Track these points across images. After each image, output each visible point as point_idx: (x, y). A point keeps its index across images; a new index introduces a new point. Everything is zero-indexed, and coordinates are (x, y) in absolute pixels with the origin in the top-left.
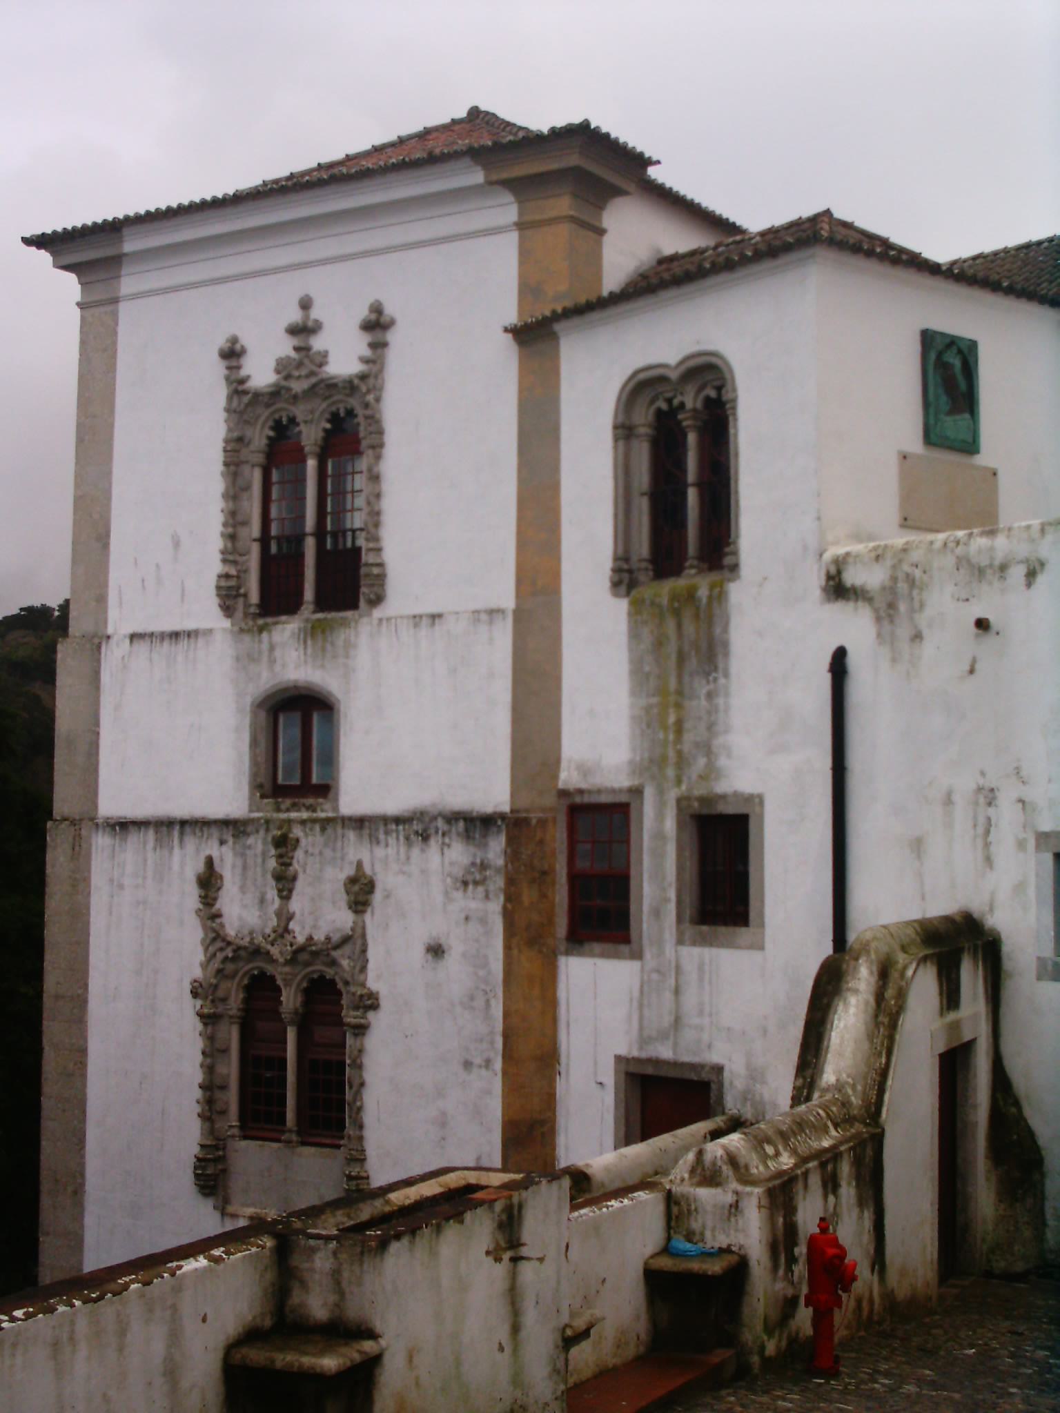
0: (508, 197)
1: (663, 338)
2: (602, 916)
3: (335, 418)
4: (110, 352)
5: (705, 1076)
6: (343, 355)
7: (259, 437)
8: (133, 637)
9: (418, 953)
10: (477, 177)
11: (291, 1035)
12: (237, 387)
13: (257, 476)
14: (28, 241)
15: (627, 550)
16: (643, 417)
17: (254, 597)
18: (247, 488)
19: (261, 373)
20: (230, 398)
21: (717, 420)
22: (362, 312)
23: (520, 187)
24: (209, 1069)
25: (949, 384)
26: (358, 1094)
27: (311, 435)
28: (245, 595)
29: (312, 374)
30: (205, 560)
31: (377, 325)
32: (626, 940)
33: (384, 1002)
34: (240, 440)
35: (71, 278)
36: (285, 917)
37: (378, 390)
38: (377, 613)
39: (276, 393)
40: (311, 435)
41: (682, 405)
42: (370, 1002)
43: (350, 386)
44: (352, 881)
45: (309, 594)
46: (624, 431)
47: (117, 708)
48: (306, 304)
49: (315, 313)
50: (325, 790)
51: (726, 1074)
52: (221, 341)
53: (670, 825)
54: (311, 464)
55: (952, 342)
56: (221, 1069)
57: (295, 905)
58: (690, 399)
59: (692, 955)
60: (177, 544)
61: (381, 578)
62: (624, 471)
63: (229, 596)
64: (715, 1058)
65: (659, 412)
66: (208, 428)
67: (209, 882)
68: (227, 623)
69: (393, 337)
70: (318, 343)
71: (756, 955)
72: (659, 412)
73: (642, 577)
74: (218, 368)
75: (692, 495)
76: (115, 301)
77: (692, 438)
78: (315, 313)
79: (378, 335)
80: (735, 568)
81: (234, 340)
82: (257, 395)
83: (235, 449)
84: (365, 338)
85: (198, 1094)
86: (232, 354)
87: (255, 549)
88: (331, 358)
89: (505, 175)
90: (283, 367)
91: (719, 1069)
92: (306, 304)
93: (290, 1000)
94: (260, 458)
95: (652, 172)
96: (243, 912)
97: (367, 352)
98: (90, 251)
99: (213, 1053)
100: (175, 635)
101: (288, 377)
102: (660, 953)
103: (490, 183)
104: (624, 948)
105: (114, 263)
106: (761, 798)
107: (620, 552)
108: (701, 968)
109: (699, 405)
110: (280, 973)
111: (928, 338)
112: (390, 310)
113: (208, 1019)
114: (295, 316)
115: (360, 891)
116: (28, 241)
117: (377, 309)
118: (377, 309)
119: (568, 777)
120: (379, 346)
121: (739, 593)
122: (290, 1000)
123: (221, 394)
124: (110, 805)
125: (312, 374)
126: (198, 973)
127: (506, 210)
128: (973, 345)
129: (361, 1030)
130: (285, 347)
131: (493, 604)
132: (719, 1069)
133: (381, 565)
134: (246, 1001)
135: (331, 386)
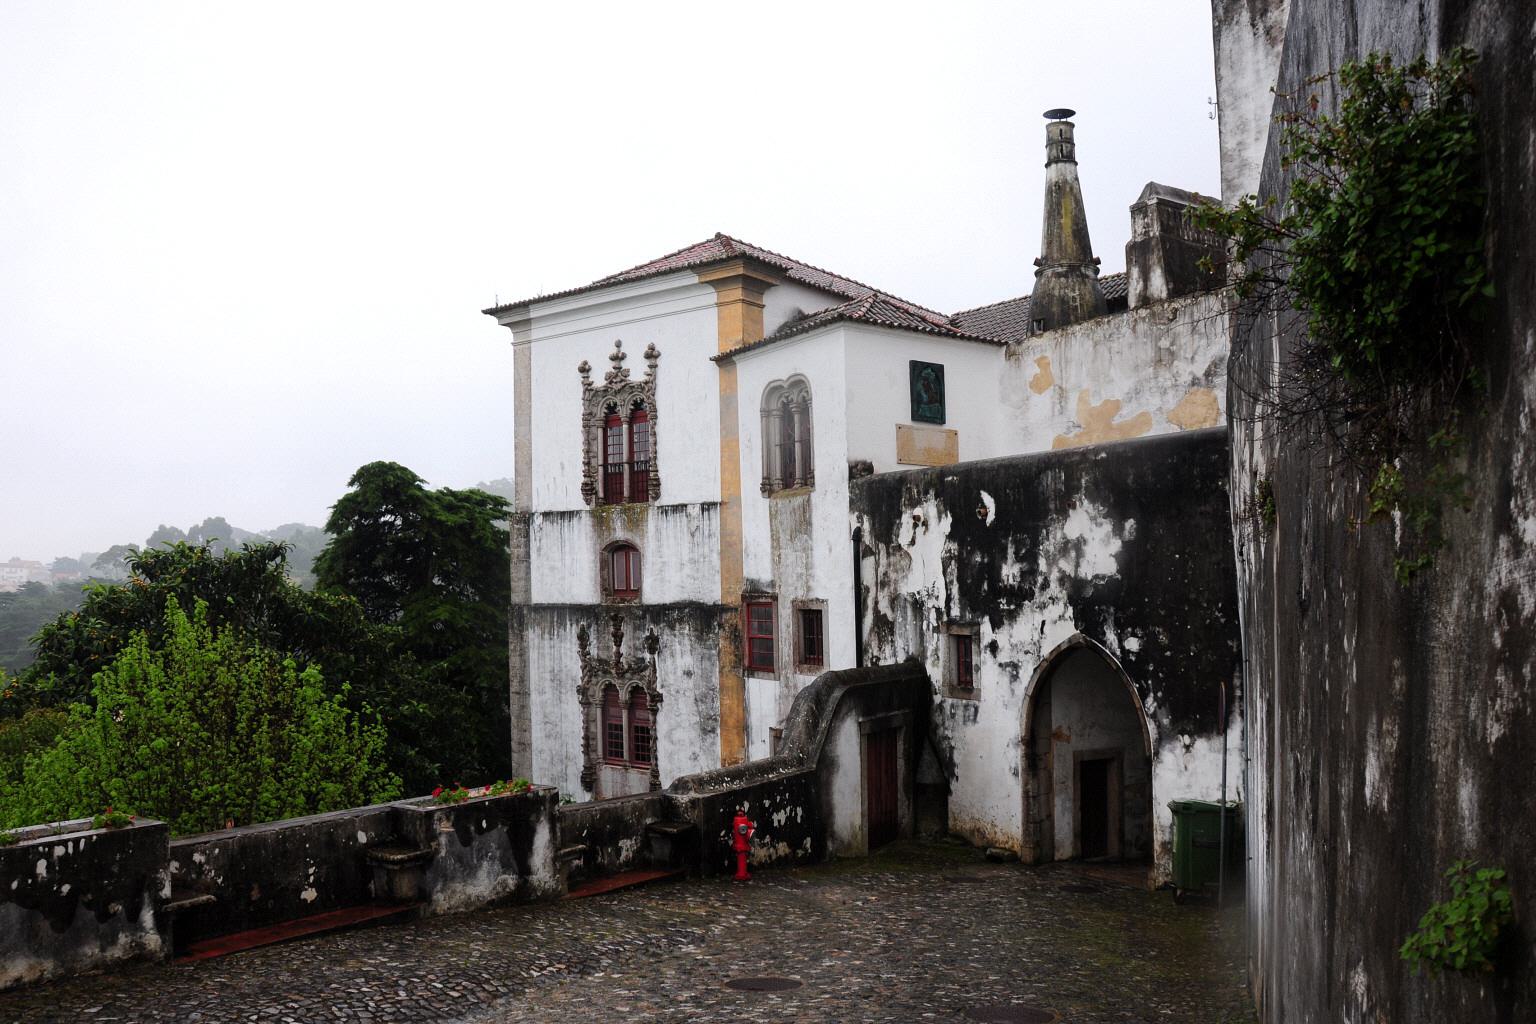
0: (711, 289)
2: (760, 661)
3: (635, 404)
4: (528, 368)
6: (637, 371)
7: (601, 412)
8: (546, 515)
9: (680, 673)
10: (695, 279)
11: (625, 714)
12: (588, 386)
13: (600, 432)
14: (485, 312)
15: (769, 474)
16: (775, 405)
17: (601, 495)
18: (596, 439)
19: (599, 380)
20: (584, 393)
21: (805, 408)
23: (717, 284)
24: (587, 729)
27: (624, 412)
28: (596, 493)
29: (622, 381)
31: (652, 355)
34: (590, 414)
35: (508, 329)
37: (652, 391)
38: (657, 503)
40: (624, 412)
43: (641, 387)
44: (647, 638)
46: (766, 413)
47: (539, 549)
48: (618, 345)
49: (623, 350)
50: (638, 592)
52: (579, 363)
54: (625, 427)
56: (593, 729)
57: (623, 649)
60: (563, 468)
63: (588, 490)
66: (576, 408)
67: (583, 639)
68: (588, 508)
69: (659, 361)
70: (625, 365)
74: (580, 376)
76: (530, 342)
78: (623, 350)
79: (653, 361)
80: (813, 485)
81: (586, 363)
83: (588, 417)
85: (582, 742)
86: (584, 369)
87: (601, 469)
88: (631, 373)
90: (610, 378)
92: (618, 345)
94: (601, 423)
97: (648, 370)
98: (514, 315)
99: (588, 722)
100: (562, 514)
101: (611, 383)
104: (771, 675)
110: (617, 682)
113: (586, 703)
114: (614, 351)
115: (653, 644)
116: (485, 312)
117: (652, 348)
118: (652, 348)
120: (653, 367)
122: (623, 695)
123: (581, 389)
124: (537, 598)
125: (622, 381)
126: (580, 683)
127: (710, 296)
129: (655, 712)
130: (609, 367)
131: (711, 500)
133: (658, 480)
134: (604, 696)
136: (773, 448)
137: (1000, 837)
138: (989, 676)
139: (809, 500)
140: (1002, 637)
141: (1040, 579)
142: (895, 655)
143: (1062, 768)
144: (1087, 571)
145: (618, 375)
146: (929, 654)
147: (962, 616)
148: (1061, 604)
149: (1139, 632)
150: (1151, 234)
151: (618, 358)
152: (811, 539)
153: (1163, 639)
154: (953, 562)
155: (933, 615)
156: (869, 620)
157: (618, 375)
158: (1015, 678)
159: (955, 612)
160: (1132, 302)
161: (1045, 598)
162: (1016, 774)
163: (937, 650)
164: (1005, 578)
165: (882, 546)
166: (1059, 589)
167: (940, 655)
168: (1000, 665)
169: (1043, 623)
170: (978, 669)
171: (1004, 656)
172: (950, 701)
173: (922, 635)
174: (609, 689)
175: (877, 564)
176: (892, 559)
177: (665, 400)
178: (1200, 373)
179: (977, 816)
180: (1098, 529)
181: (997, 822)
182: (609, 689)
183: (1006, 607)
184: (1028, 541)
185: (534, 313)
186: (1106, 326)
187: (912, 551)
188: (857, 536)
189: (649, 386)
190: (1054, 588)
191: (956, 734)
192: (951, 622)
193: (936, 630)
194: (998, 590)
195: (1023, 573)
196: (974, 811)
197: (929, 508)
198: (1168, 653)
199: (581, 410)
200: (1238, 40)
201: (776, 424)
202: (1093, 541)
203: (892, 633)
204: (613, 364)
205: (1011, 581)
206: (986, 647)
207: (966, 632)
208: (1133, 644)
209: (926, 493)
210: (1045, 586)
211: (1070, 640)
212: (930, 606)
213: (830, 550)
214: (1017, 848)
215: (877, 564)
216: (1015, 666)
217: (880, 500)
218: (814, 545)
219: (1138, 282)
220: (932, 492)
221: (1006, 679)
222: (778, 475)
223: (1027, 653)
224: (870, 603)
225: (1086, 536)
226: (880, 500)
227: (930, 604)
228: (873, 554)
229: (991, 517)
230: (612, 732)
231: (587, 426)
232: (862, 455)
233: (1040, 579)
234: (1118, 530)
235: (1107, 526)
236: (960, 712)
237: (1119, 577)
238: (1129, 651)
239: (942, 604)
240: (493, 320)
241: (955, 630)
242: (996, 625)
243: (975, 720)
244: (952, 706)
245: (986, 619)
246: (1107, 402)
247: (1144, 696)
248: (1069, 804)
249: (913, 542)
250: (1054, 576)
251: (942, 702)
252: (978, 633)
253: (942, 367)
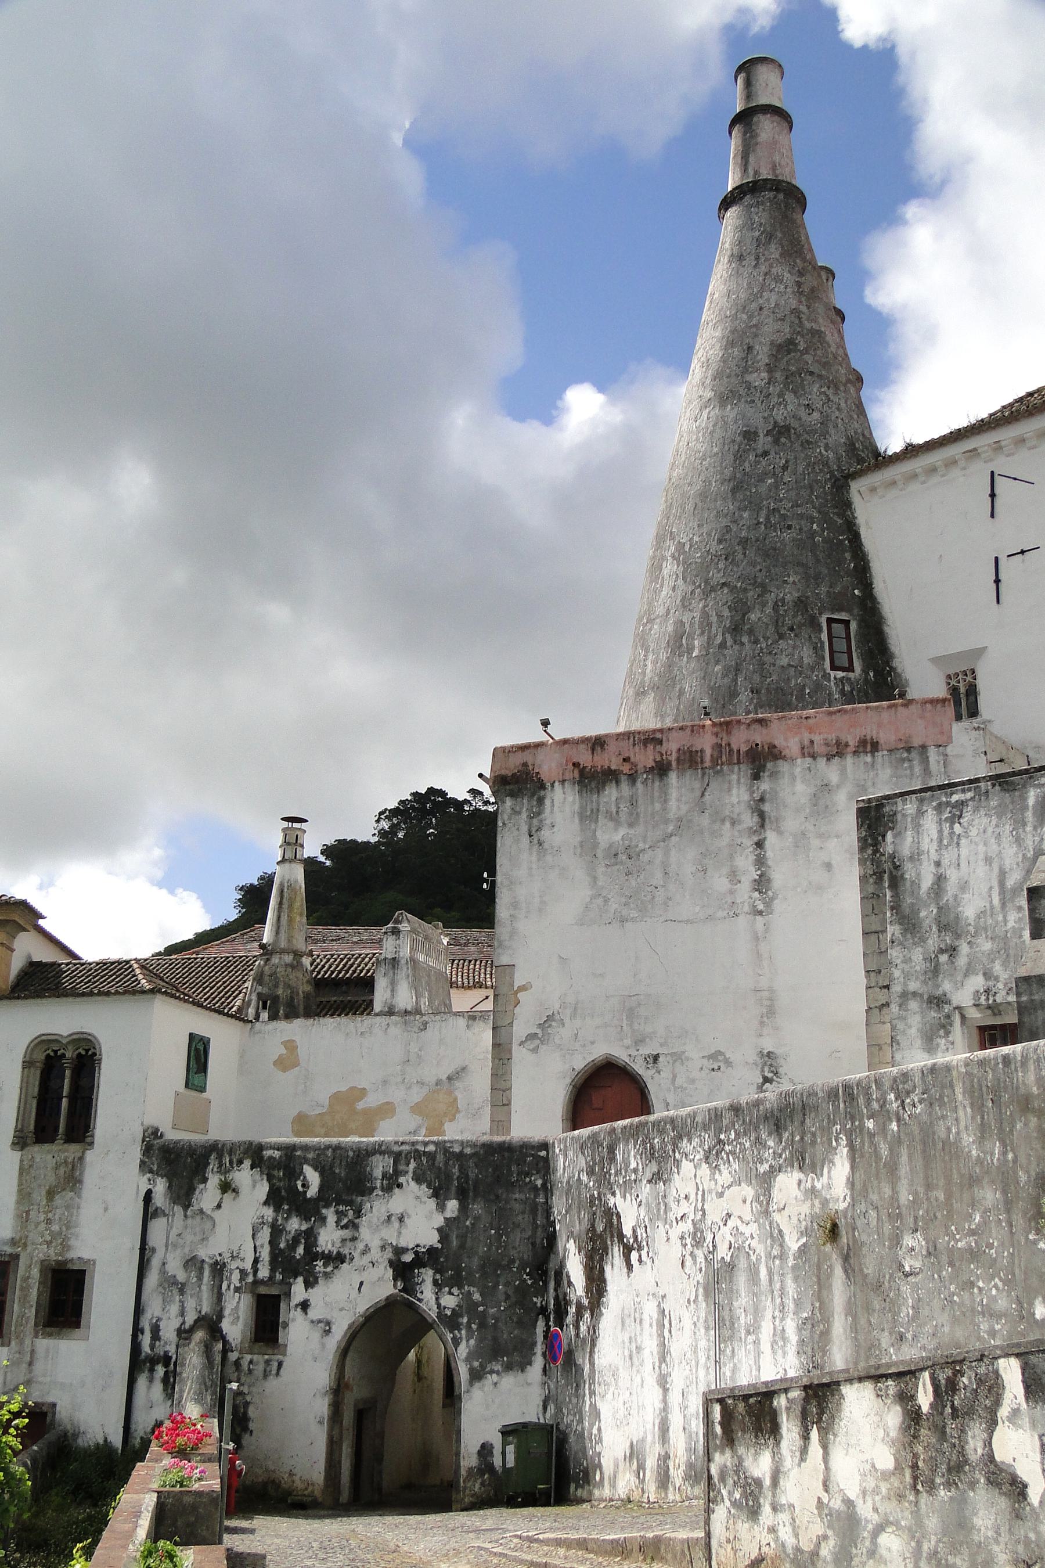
1: (59, 1019)
5: (44, 1409)
41: (64, 1055)
46: (27, 1064)
51: (58, 1408)
53: (35, 1272)
59: (43, 1344)
62: (25, 1083)
64: (50, 1399)
65: (48, 1056)
71: (82, 1344)
72: (48, 1056)
73: (29, 1141)
77: (68, 1073)
91: (54, 1405)
95: (41, 922)
102: (21, 1343)
106: (94, 1261)
107: (19, 1126)
108: (47, 1351)
109: (75, 1056)
121: (90, 1156)
132: (54, 1405)
136: (29, 1098)
137: (298, 1484)
138: (297, 1332)
139: (81, 1159)
140: (315, 1296)
141: (361, 1246)
142: (182, 1314)
143: (348, 1417)
144: (408, 1240)
146: (227, 1313)
147: (271, 1278)
148: (382, 1267)
149: (455, 1290)
150: (401, 954)
152: (79, 1197)
153: (477, 1297)
154: (265, 1227)
155: (236, 1277)
156: (152, 1279)
158: (328, 1332)
159: (264, 1273)
160: (378, 1007)
161: (366, 1259)
162: (321, 1423)
163: (237, 1308)
164: (324, 1244)
165: (178, 1209)
166: (380, 1254)
167: (241, 1314)
168: (312, 1322)
169: (361, 1283)
170: (286, 1325)
171: (314, 1313)
172: (248, 1357)
173: (220, 1296)
175: (170, 1226)
176: (189, 1221)
178: (444, 1077)
179: (272, 1468)
180: (423, 1206)
181: (294, 1471)
183: (322, 1269)
184: (351, 1213)
186: (359, 1025)
187: (217, 1215)
188: (148, 1197)
190: (375, 1254)
191: (254, 1389)
192: (256, 1282)
193: (237, 1290)
194: (312, 1255)
195: (344, 1241)
196: (270, 1463)
197: (244, 1176)
198: (481, 1309)
200: (517, 841)
201: (36, 1075)
202: (416, 1218)
203: (182, 1292)
205: (330, 1247)
206: (297, 1306)
207: (274, 1291)
208: (450, 1301)
209: (240, 1162)
210: (366, 1250)
211: (387, 1298)
212: (233, 1267)
213: (106, 1209)
214: (317, 1493)
215: (170, 1226)
216: (328, 1323)
217: (180, 1166)
218: (83, 1205)
219: (385, 991)
220: (247, 1163)
221: (316, 1335)
222: (32, 1127)
223: (341, 1310)
224: (155, 1263)
225: (410, 1212)
226: (180, 1166)
227: (233, 1265)
228: (165, 1215)
229: (312, 1192)
232: (151, 1120)
233: (361, 1246)
234: (441, 1207)
235: (432, 1203)
236: (259, 1369)
237: (440, 1246)
238: (445, 1308)
239: (248, 1265)
241: (263, 1290)
242: (308, 1285)
243: (278, 1374)
244: (251, 1362)
245: (300, 1279)
246: (352, 1088)
247: (456, 1342)
248: (349, 1450)
249: (219, 1206)
250: (375, 1244)
251: (239, 1359)
252: (288, 1294)
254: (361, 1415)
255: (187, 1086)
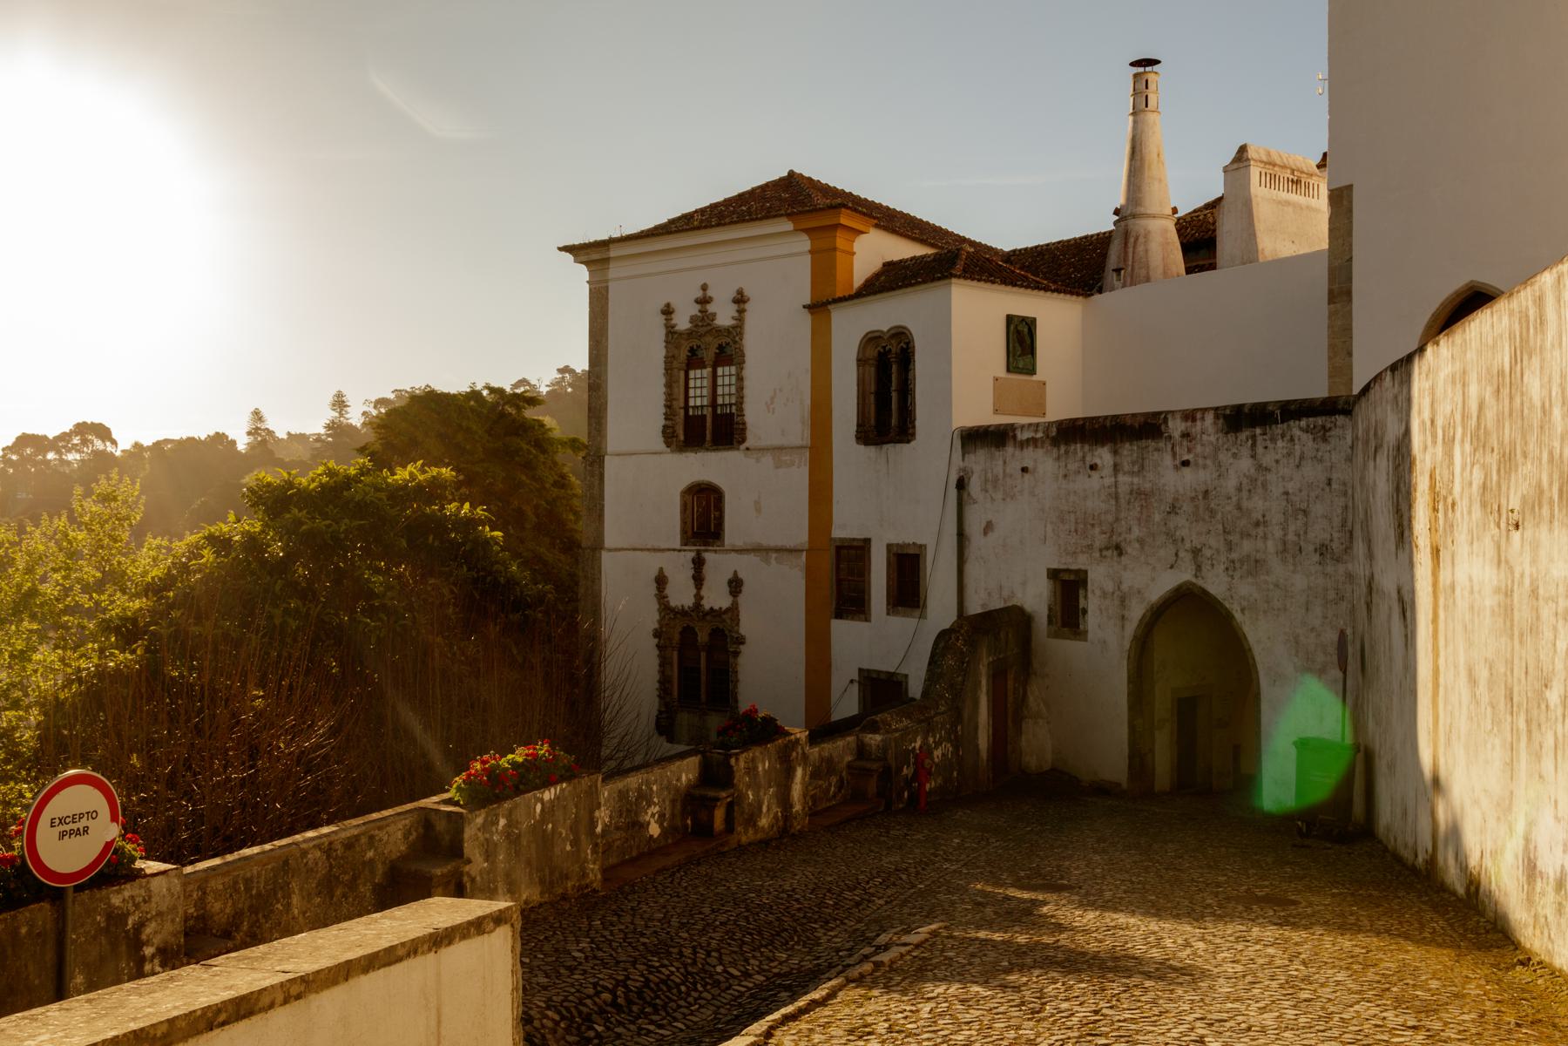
1: (884, 314)
2: (852, 603)
6: (724, 316)
7: (683, 354)
10: (789, 226)
11: (703, 655)
12: (671, 331)
13: (682, 374)
16: (872, 353)
17: (682, 438)
19: (682, 323)
21: (906, 356)
22: (732, 294)
24: (662, 672)
25: (1021, 341)
26: (736, 687)
30: (655, 419)
31: (740, 300)
32: (863, 612)
33: (748, 641)
36: (699, 597)
37: (741, 334)
39: (690, 334)
40: (709, 355)
42: (741, 641)
43: (728, 331)
45: (708, 436)
46: (861, 362)
48: (704, 288)
52: (661, 305)
55: (1023, 319)
58: (894, 347)
61: (744, 430)
62: (861, 382)
66: (658, 352)
69: (747, 306)
70: (711, 308)
74: (661, 319)
75: (894, 395)
78: (709, 293)
81: (668, 305)
82: (681, 334)
84: (735, 307)
86: (668, 311)
87: (682, 412)
89: (804, 226)
90: (693, 319)
92: (704, 288)
93: (703, 637)
96: (681, 595)
98: (592, 254)
99: (664, 663)
103: (796, 230)
105: (607, 260)
111: (1010, 319)
112: (746, 293)
114: (700, 294)
115: (735, 585)
117: (740, 292)
118: (740, 292)
119: (837, 533)
120: (741, 312)
122: (703, 637)
123: (663, 331)
128: (1034, 320)
129: (737, 654)
130: (695, 310)
135: (719, 331)
145: (703, 320)
151: (704, 301)
157: (703, 320)
174: (688, 632)
177: (753, 344)
182: (688, 632)
185: (614, 252)
189: (737, 331)
199: (663, 352)
201: (871, 371)
204: (698, 307)
222: (873, 422)
230: (688, 673)
231: (668, 370)
240: (569, 257)
253: (1034, 320)
254: (1186, 709)
255: (1008, 370)
